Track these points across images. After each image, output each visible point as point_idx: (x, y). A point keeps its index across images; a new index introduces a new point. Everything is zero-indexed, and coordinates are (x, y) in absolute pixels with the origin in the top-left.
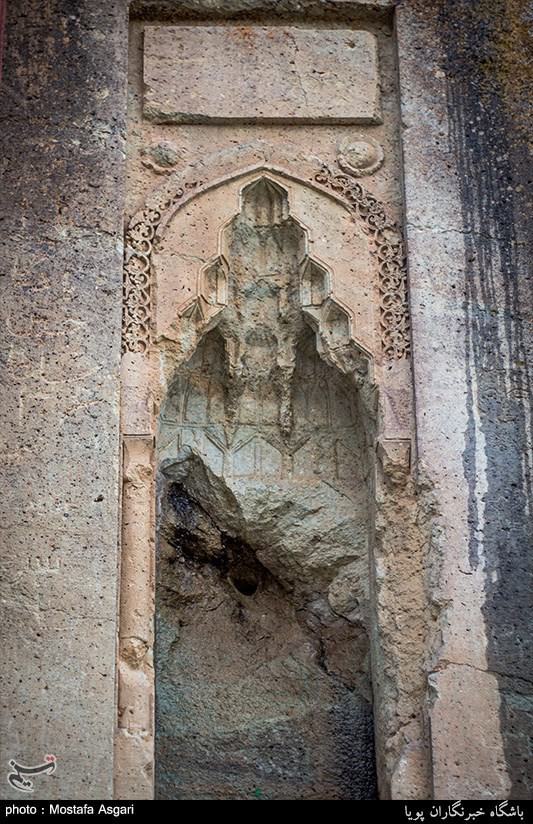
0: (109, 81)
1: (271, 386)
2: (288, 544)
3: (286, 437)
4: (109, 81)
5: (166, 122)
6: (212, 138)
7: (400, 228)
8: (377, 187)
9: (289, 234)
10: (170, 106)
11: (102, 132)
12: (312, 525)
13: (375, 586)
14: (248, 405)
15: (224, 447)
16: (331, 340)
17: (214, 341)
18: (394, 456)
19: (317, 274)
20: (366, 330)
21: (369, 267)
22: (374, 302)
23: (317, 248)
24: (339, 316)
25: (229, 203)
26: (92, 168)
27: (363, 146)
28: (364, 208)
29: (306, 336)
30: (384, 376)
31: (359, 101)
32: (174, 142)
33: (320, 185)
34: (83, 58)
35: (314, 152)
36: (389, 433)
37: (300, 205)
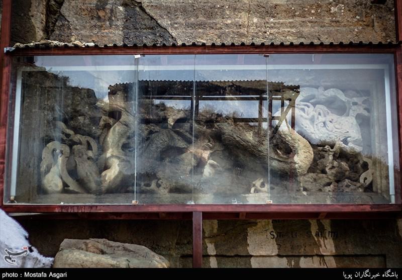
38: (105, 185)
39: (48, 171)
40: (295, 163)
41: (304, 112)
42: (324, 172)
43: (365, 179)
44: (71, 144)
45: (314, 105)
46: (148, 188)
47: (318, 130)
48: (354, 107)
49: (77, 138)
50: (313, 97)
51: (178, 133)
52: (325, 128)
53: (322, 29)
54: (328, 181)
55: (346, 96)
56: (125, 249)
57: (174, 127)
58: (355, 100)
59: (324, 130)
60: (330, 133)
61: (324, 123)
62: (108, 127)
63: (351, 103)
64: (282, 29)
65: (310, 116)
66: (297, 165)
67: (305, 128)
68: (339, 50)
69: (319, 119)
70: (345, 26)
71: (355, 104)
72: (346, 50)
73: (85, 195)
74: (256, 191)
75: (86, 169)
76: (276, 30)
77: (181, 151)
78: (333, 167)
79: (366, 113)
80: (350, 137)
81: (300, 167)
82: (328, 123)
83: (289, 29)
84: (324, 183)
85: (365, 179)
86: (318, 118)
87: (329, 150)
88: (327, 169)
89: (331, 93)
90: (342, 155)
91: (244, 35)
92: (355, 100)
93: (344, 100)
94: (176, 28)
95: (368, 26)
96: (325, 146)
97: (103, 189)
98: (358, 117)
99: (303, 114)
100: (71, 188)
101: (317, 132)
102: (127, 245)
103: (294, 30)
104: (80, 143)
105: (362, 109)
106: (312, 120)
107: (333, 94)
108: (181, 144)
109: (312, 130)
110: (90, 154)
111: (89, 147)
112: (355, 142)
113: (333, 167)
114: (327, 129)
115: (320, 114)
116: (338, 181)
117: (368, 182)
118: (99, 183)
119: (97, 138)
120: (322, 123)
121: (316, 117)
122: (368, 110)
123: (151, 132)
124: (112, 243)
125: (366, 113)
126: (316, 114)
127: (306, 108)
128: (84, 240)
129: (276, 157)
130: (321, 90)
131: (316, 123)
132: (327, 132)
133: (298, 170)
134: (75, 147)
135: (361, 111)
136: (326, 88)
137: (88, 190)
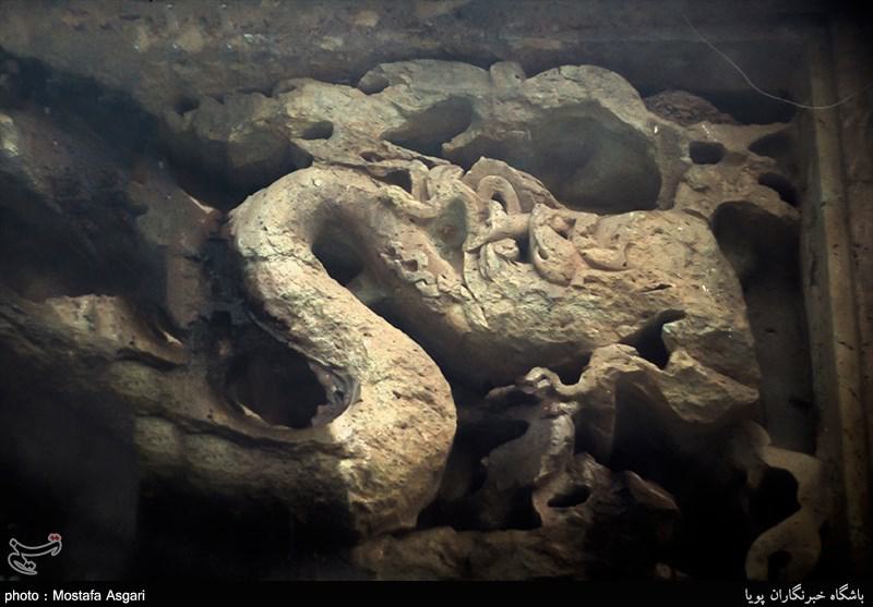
40: (338, 451)
41: (407, 186)
47: (487, 279)
48: (698, 174)
50: (459, 113)
52: (523, 267)
55: (649, 108)
58: (709, 132)
60: (558, 291)
63: (685, 146)
66: (346, 465)
67: (406, 272)
69: (493, 217)
71: (707, 154)
78: (576, 496)
80: (677, 315)
81: (366, 474)
86: (485, 215)
87: (551, 392)
88: (540, 505)
89: (564, 86)
92: (709, 132)
93: (639, 125)
98: (729, 224)
101: (479, 290)
105: (748, 179)
106: (452, 232)
107: (576, 92)
109: (451, 282)
112: (712, 346)
114: (537, 271)
120: (511, 243)
121: (472, 212)
129: (220, 419)
130: (507, 78)
131: (477, 242)
132: (539, 284)
133: (353, 497)
135: (742, 187)
136: (534, 66)
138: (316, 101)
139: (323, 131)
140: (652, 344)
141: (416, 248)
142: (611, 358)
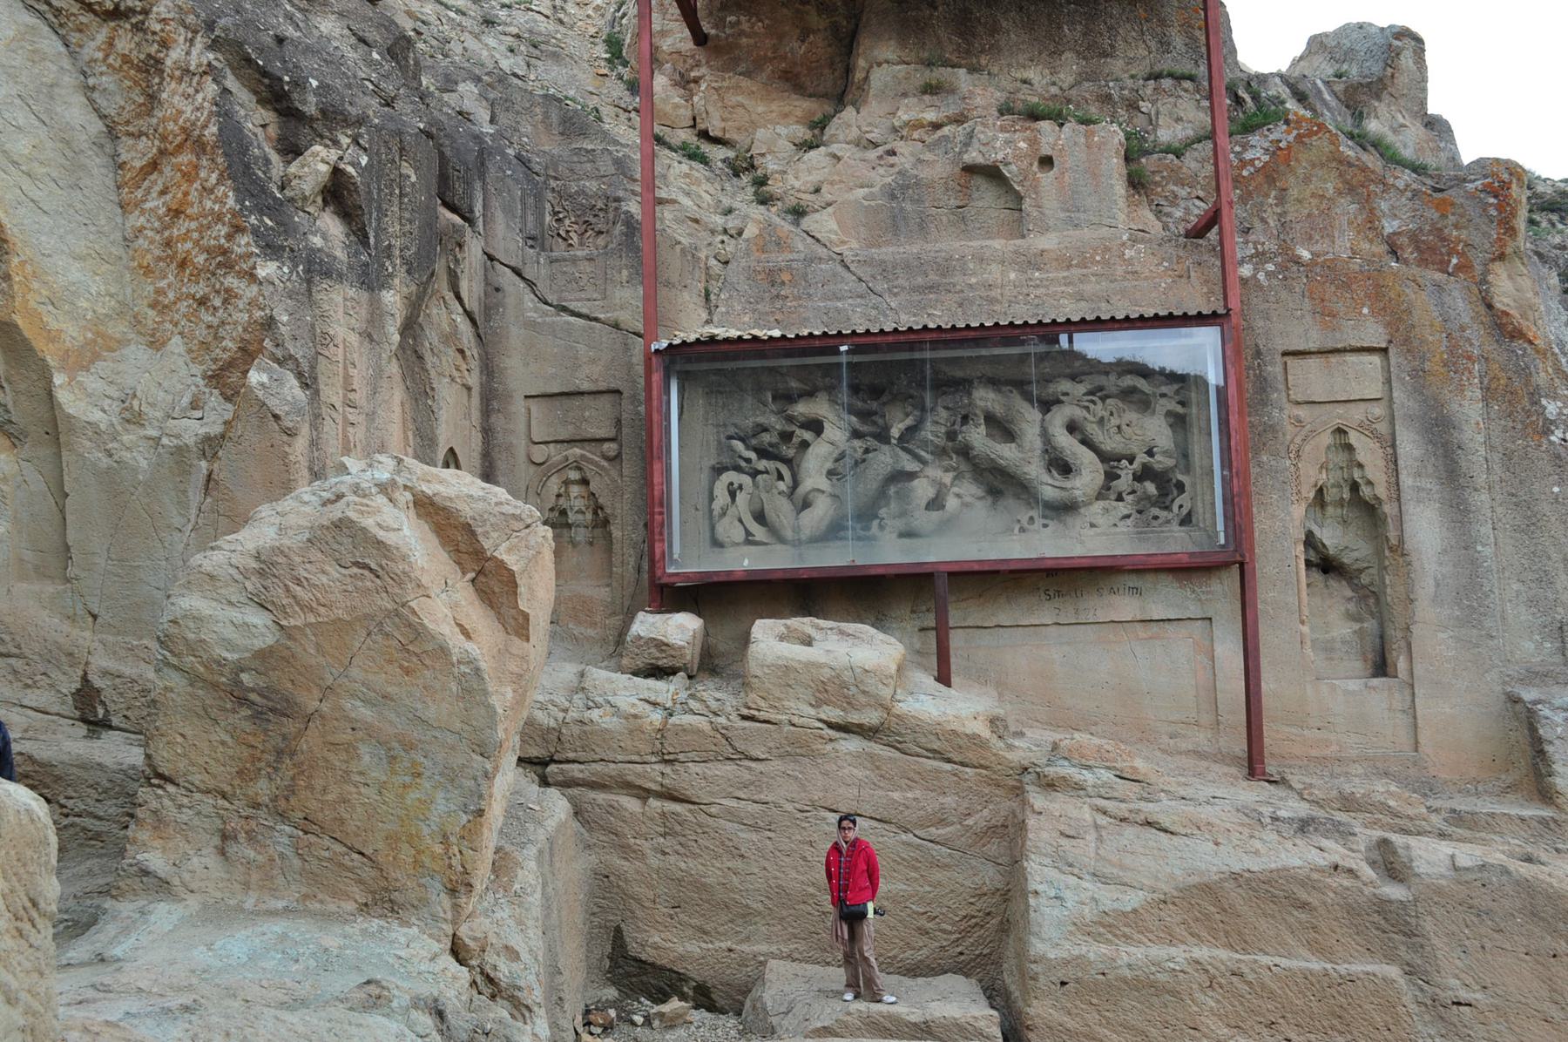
0: (1277, 390)
1: (1341, 503)
2: (1345, 561)
3: (1344, 522)
4: (1277, 390)
5: (1298, 403)
6: (1318, 409)
7: (1393, 446)
8: (1383, 428)
9: (1349, 448)
10: (1300, 398)
11: (1276, 413)
12: (1356, 555)
13: (1385, 587)
14: (1330, 510)
15: (1321, 526)
16: (1365, 491)
17: (1320, 491)
18: (1394, 541)
19: (1360, 466)
20: (1381, 491)
21: (1381, 463)
22: (1384, 478)
23: (1361, 456)
24: (1370, 483)
25: (1327, 439)
26: (1272, 429)
27: (1378, 410)
28: (1378, 437)
29: (1355, 487)
30: (1388, 509)
31: (1374, 389)
32: (1302, 412)
33: (1361, 428)
34: (1265, 379)
35: (1357, 414)
36: (1392, 535)
37: (1354, 438)
38: (806, 533)
39: (724, 514)
41: (1089, 411)
42: (1120, 498)
43: (1181, 506)
44: (755, 474)
45: (1103, 399)
46: (867, 533)
48: (1163, 401)
49: (763, 464)
50: (1101, 389)
51: (904, 449)
53: (1113, 286)
54: (1126, 512)
55: (1149, 383)
56: (842, 633)
57: (900, 439)
58: (1164, 389)
59: (1118, 438)
61: (1119, 427)
62: (805, 445)
64: (1052, 289)
65: (1097, 419)
68: (1139, 324)
70: (1146, 278)
71: (1163, 395)
72: (1150, 324)
73: (779, 547)
74: (1022, 530)
75: (780, 510)
76: (1043, 290)
77: (912, 476)
79: (1179, 409)
82: (1124, 427)
83: (1063, 288)
84: (1120, 515)
85: (1181, 506)
90: (1145, 474)
91: (997, 301)
92: (1164, 389)
94: (895, 295)
95: (1181, 277)
96: (1119, 461)
97: (803, 537)
98: (1169, 414)
99: (1087, 416)
100: (757, 538)
101: (1109, 441)
102: (844, 626)
103: (1070, 290)
104: (767, 472)
106: (1101, 421)
108: (910, 465)
110: (782, 486)
111: (780, 477)
112: (1166, 453)
113: (1133, 492)
115: (1112, 414)
116: (1140, 512)
117: (1185, 511)
118: (797, 529)
119: (788, 462)
122: (1182, 403)
123: (867, 451)
124: (821, 622)
125: (1179, 409)
126: (1106, 414)
127: (1092, 406)
128: (783, 621)
134: (759, 477)
137: (782, 540)
138: (1065, 385)
139: (1066, 394)
140: (1150, 453)
141: (1092, 429)
142: (1142, 458)
